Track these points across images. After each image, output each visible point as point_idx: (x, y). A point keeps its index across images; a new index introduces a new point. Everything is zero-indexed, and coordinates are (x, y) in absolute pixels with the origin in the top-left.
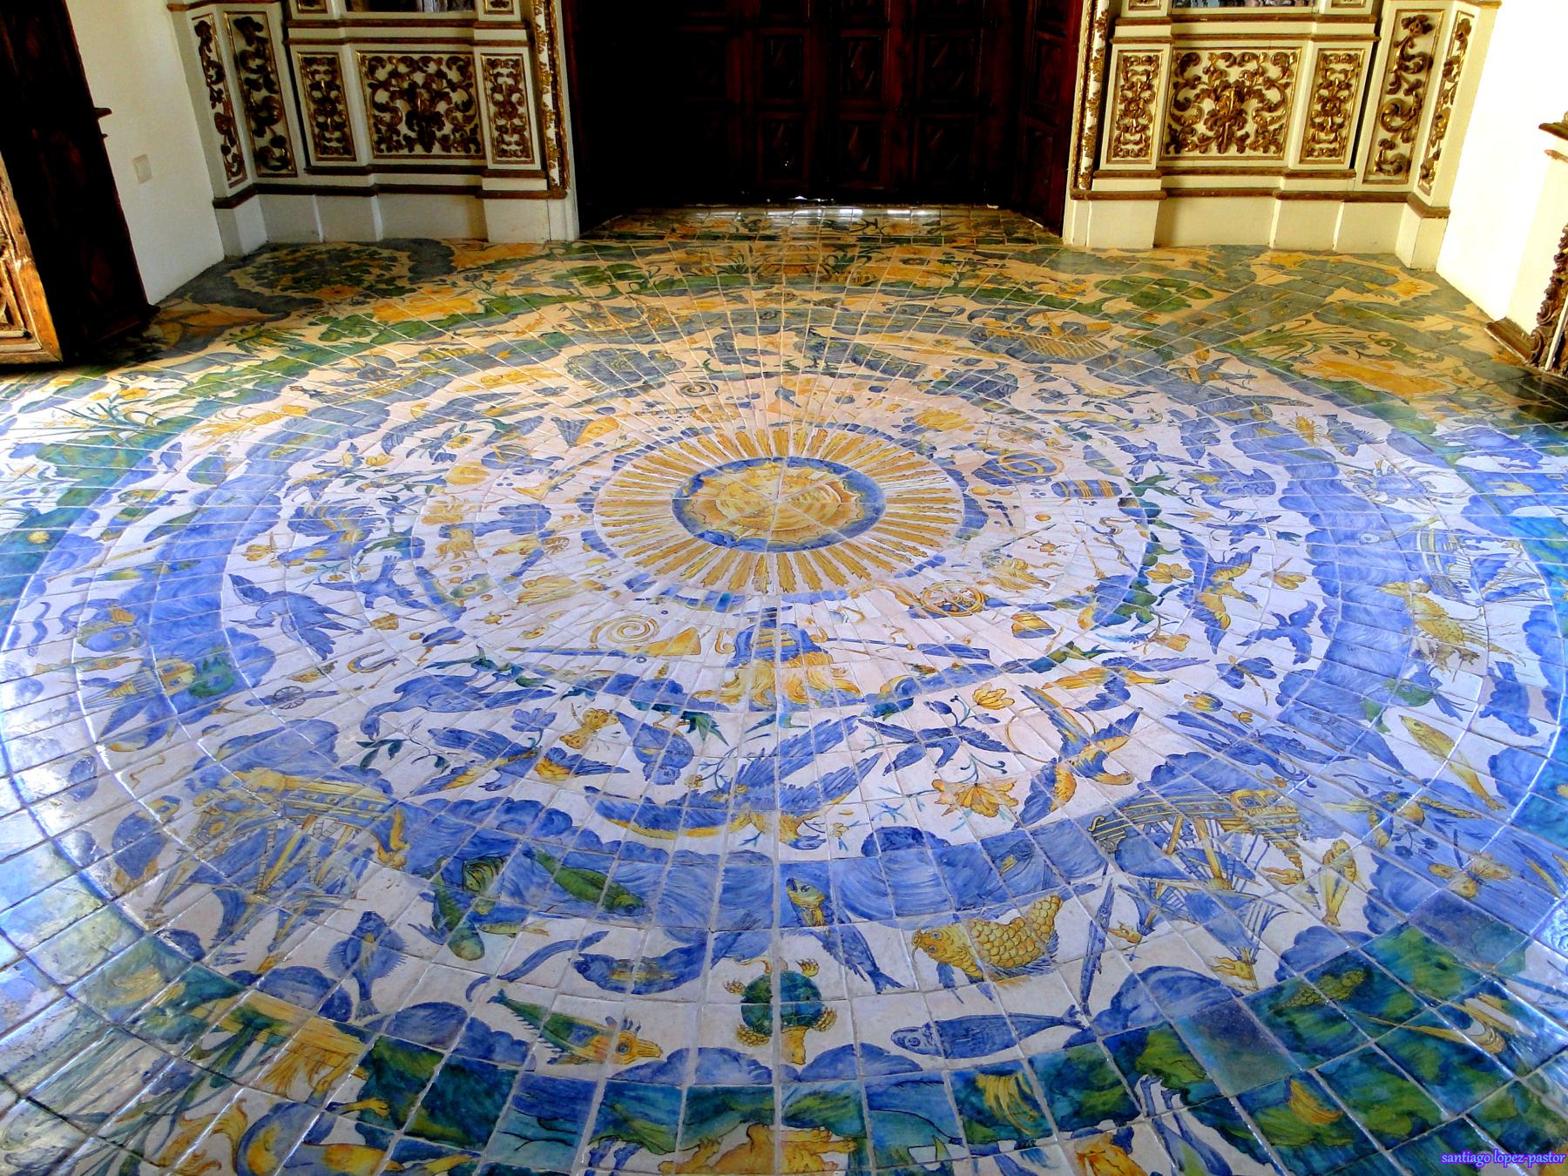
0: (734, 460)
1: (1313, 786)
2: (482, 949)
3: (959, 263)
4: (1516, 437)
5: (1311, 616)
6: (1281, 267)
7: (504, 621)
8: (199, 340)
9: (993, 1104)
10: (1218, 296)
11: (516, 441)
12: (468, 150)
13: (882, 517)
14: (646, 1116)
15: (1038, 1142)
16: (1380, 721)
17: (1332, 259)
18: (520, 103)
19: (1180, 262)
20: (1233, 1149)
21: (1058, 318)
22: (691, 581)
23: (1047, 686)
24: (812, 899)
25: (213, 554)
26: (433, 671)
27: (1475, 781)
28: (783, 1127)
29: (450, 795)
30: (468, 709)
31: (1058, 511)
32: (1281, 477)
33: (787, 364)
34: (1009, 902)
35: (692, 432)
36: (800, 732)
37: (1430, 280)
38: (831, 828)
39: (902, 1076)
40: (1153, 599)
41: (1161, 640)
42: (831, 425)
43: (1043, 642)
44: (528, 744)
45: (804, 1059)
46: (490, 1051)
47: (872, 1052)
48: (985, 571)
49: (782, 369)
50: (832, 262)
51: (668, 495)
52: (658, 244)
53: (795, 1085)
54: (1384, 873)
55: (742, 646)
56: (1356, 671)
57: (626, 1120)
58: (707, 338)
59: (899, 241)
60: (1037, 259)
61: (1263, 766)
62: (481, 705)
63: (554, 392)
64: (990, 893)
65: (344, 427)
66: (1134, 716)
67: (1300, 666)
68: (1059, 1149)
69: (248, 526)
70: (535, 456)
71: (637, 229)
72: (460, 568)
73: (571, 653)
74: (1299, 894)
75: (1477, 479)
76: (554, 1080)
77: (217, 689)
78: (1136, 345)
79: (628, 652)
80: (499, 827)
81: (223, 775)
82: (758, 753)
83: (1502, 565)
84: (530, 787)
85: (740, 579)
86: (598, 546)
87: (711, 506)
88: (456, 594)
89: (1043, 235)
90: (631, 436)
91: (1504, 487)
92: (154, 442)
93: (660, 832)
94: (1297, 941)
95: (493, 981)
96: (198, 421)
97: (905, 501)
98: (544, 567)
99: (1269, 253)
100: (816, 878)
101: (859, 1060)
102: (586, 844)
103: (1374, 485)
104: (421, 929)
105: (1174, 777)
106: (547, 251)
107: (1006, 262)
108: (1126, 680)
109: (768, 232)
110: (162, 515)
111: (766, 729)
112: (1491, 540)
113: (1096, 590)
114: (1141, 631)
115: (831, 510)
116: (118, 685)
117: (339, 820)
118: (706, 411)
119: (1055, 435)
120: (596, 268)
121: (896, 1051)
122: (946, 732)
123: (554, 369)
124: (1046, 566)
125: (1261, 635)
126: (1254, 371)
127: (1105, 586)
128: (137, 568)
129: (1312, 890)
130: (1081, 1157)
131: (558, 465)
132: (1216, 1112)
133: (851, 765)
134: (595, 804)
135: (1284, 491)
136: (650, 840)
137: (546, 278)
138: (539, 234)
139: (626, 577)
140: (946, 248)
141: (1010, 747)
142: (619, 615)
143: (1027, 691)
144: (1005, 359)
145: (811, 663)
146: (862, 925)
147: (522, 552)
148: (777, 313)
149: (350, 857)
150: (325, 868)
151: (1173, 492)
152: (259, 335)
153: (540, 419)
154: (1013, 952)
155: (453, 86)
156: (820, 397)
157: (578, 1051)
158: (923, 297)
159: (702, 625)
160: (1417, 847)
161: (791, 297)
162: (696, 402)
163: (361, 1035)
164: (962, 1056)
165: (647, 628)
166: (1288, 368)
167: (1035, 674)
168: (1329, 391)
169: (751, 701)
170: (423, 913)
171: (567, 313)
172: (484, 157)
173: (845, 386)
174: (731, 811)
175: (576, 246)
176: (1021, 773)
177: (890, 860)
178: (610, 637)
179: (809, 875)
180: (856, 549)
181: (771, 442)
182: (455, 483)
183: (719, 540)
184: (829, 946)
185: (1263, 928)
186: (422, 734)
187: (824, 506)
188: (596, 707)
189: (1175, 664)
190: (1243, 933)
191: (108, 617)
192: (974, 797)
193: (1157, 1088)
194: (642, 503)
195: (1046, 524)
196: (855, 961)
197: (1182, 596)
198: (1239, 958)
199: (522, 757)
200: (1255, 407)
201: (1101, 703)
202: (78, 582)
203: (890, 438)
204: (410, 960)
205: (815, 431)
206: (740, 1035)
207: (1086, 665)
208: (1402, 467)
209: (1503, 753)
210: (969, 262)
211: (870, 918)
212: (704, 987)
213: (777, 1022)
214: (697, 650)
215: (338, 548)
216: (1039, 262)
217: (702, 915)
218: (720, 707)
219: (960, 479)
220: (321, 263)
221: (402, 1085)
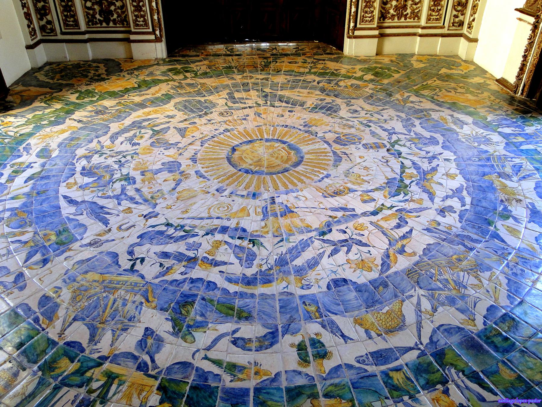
0: (245, 140)
1: (479, 252)
2: (194, 339)
3: (309, 63)
4: (515, 120)
5: (463, 189)
6: (421, 61)
7: (173, 207)
8: (28, 102)
9: (397, 382)
10: (402, 72)
13: (304, 160)
14: (272, 400)
15: (417, 395)
16: (495, 227)
17: (437, 57)
19: (386, 60)
20: (485, 391)
21: (350, 82)
22: (240, 188)
23: (378, 221)
24: (313, 308)
25: (52, 187)
26: (150, 229)
27: (533, 248)
28: (323, 399)
29: (168, 278)
31: (365, 155)
32: (441, 139)
33: (256, 103)
34: (384, 304)
35: (227, 130)
36: (294, 244)
37: (471, 64)
38: (314, 280)
39: (362, 375)
40: (406, 186)
41: (413, 201)
42: (278, 126)
43: (373, 204)
44: (193, 256)
45: (325, 371)
46: (206, 379)
47: (350, 367)
48: (346, 179)
49: (255, 105)
50: (263, 63)
51: (224, 154)
52: (198, 58)
53: (324, 382)
54: (510, 282)
55: (265, 212)
56: (483, 209)
57: (264, 402)
58: (224, 94)
59: (286, 55)
60: (336, 60)
61: (460, 246)
63: (172, 117)
64: (377, 301)
65: (94, 134)
66: (411, 231)
67: (463, 208)
68: (424, 397)
69: (64, 175)
70: (170, 142)
71: (188, 53)
72: (151, 188)
73: (202, 219)
74: (484, 293)
75: (505, 136)
76: (234, 389)
77: (67, 241)
78: (378, 91)
79: (223, 217)
80: (190, 289)
81: (77, 276)
82: (280, 253)
83: (521, 167)
84: (197, 273)
85: (258, 187)
87: (241, 158)
88: (152, 198)
89: (336, 51)
90: (205, 133)
91: (515, 138)
92: (20, 143)
93: (251, 287)
94: (487, 311)
95: (201, 351)
96: (35, 134)
97: (311, 153)
99: (416, 56)
100: (313, 300)
101: (344, 369)
102: (224, 294)
103: (472, 140)
104: (168, 332)
105: (431, 252)
106: (156, 62)
107: (326, 62)
108: (405, 217)
109: (237, 53)
110: (29, 173)
111: (281, 244)
112: (515, 158)
113: (387, 184)
114: (406, 198)
115: (285, 158)
116: (26, 243)
117: (127, 291)
118: (230, 122)
119: (358, 126)
120: (176, 68)
121: (358, 365)
122: (346, 241)
123: (170, 108)
124: (367, 175)
125: (447, 197)
126: (421, 100)
127: (390, 182)
128: (24, 194)
129: (488, 291)
130: (433, 400)
131: (180, 145)
132: (474, 377)
133: (315, 256)
134: (224, 278)
135: (442, 143)
136: (248, 290)
137: (158, 73)
138: (153, 56)
139: (216, 187)
140: (303, 57)
141: (370, 245)
142: (216, 203)
143: (371, 223)
144: (334, 98)
145: (292, 217)
146: (334, 317)
147: (174, 180)
148: (248, 83)
149: (135, 306)
150: (126, 312)
151: (404, 145)
152: (52, 99)
154: (390, 323)
156: (271, 115)
157: (240, 376)
158: (299, 76)
159: (248, 205)
160: (519, 272)
161: (251, 78)
162: (225, 119)
163: (156, 378)
164: (382, 365)
165: (228, 208)
166: (433, 98)
167: (373, 216)
168: (448, 106)
169: (273, 233)
170: (168, 326)
171: (170, 86)
173: (279, 111)
174: (275, 277)
175: (167, 60)
176: (377, 254)
177: (338, 291)
178: (215, 212)
179: (310, 299)
180: (298, 172)
181: (257, 133)
182: (142, 154)
183: (247, 172)
184: (324, 326)
185: (475, 307)
186: (151, 254)
187: (282, 157)
189: (421, 210)
190: (468, 309)
191: (16, 215)
192: (362, 265)
193: (453, 371)
194: (215, 159)
195: (363, 160)
196: (335, 331)
197: (417, 184)
198: (469, 319)
199: (192, 261)
200: (425, 113)
201: (398, 226)
203: (300, 130)
204: (168, 346)
205: (272, 128)
206: (299, 364)
207: (389, 212)
208: (480, 133)
209: (539, 235)
210: (313, 62)
211: (336, 314)
212: (282, 345)
213: (311, 358)
214: (249, 215)
215: (102, 182)
216: (337, 62)
217: (274, 318)
218: (262, 236)
219: (329, 144)
220: (69, 69)
221: (175, 396)
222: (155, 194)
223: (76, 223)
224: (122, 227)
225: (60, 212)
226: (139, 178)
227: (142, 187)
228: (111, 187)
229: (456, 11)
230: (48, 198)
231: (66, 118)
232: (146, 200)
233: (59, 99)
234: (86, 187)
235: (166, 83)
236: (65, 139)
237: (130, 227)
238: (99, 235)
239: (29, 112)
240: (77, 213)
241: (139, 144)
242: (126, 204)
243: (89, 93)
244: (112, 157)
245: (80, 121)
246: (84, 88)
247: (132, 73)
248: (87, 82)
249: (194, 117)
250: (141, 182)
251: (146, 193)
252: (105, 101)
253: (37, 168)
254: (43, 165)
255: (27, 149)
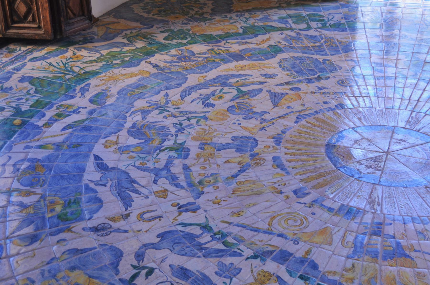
7: (223, 203)
11: (246, 100)
26: (180, 228)
30: (193, 256)
62: (200, 254)
63: (271, 77)
70: (255, 110)
86: (280, 166)
88: (200, 183)
98: (250, 174)
131: (266, 116)
137: (275, 18)
147: (239, 163)
153: (261, 90)
171: (284, 36)
186: (166, 266)
188: (265, 268)
202: (27, 147)
222: (207, 179)
223: (93, 195)
224: (145, 216)
225: (82, 175)
226: (194, 149)
227: (193, 165)
228: (155, 155)
230: (77, 155)
231: (142, 60)
232: (191, 185)
233: (144, 37)
234: (126, 150)
235: (279, 32)
236: (130, 86)
237: (155, 218)
238: (112, 219)
239: (106, 47)
240: (101, 183)
241: (213, 105)
242: (164, 183)
243: (182, 34)
244: (174, 116)
245: (156, 66)
246: (176, 28)
247: (241, 15)
248: (185, 21)
249: (300, 81)
250: (195, 157)
251: (195, 174)
252: (196, 45)
253: (82, 116)
254: (91, 113)
255: (83, 91)
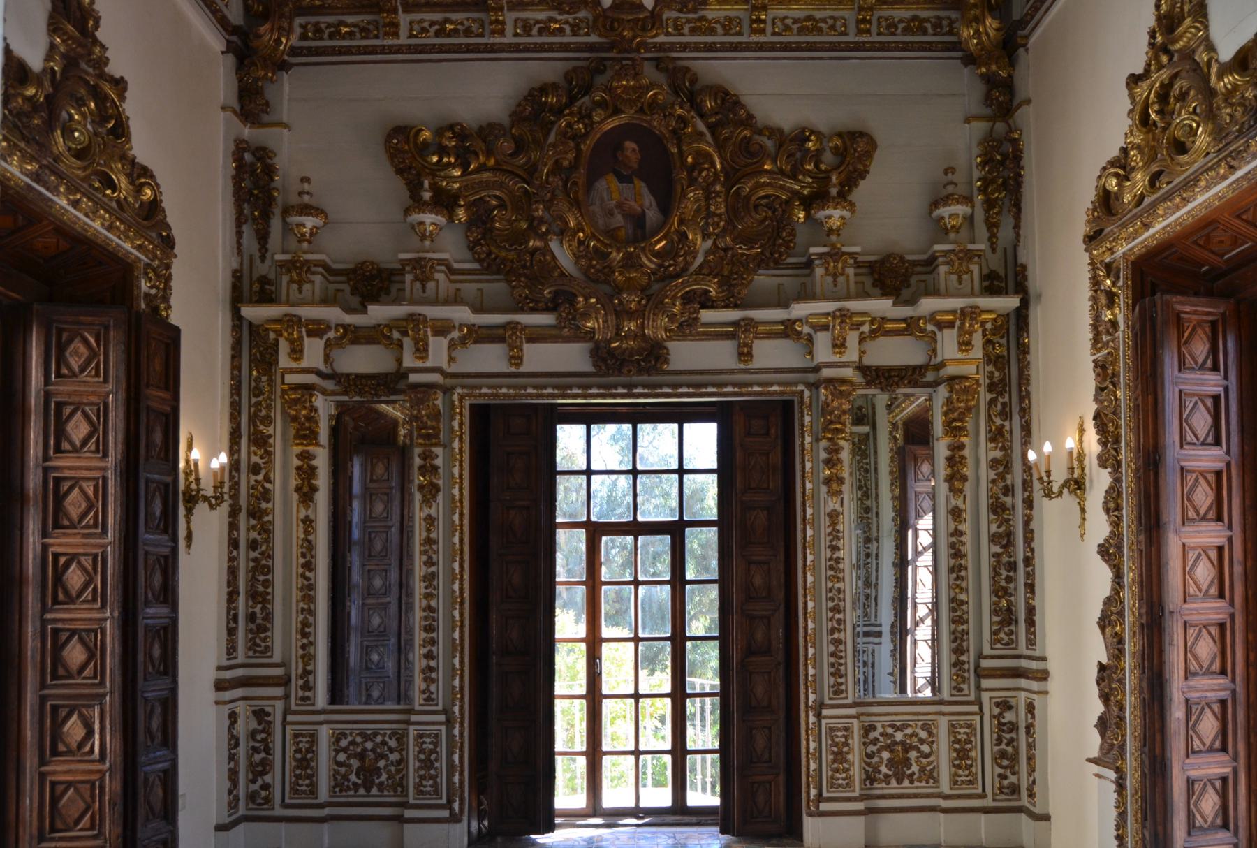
12: (395, 791)
18: (436, 760)
155: (391, 750)
172: (407, 796)
229: (1002, 767)
